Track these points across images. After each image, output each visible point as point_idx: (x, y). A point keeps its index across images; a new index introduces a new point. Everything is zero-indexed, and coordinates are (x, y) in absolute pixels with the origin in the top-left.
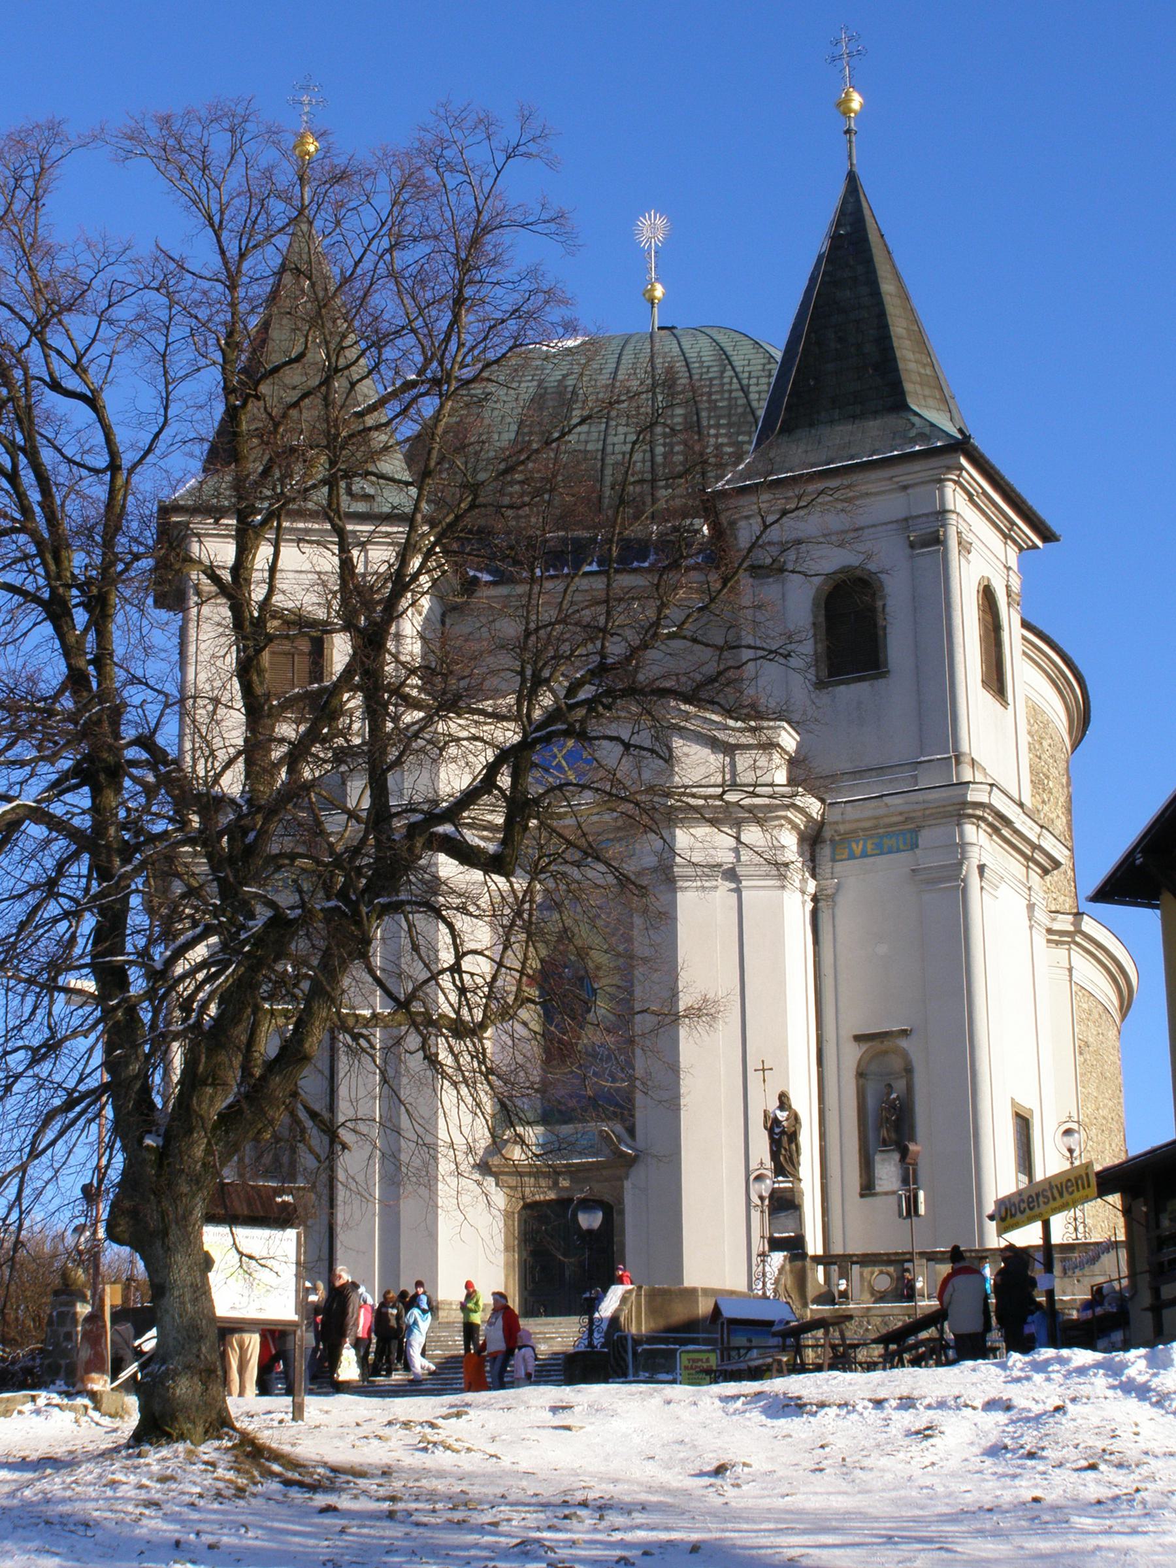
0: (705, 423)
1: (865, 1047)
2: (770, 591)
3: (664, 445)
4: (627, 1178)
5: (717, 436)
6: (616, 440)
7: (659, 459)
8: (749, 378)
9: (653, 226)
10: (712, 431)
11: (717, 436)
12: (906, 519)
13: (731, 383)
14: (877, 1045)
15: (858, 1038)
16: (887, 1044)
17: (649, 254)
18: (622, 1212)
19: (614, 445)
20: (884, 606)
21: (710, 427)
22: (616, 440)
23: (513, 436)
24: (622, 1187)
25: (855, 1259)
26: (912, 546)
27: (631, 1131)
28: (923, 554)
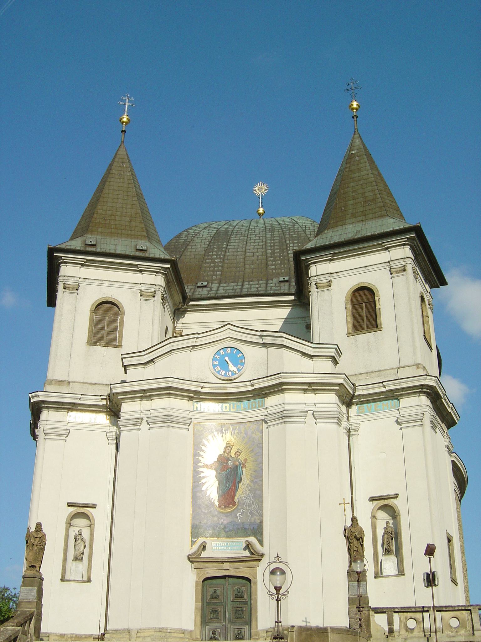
0: (288, 242)
1: (375, 503)
2: (325, 294)
3: (271, 249)
5: (294, 246)
6: (250, 248)
7: (269, 255)
8: (306, 227)
9: (261, 190)
10: (291, 245)
11: (294, 246)
12: (389, 262)
13: (298, 229)
14: (382, 503)
15: (372, 499)
16: (386, 502)
17: (259, 198)
18: (256, 583)
19: (249, 249)
20: (379, 299)
21: (290, 243)
22: (250, 248)
23: (206, 246)
25: (396, 610)
26: (391, 274)
27: (261, 542)
28: (397, 276)
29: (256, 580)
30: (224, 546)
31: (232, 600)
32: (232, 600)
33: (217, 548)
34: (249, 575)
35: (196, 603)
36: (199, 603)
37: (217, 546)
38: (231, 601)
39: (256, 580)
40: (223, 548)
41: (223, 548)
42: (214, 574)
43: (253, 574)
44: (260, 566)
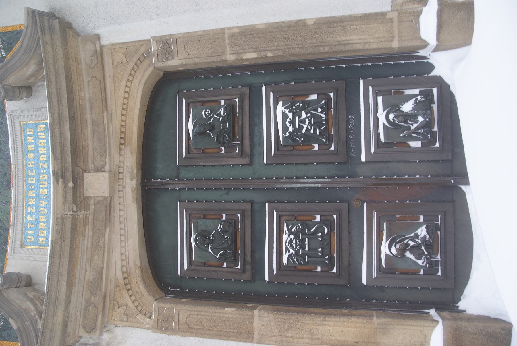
4: (98, 37)
24: (113, 47)
29: (154, 46)
30: (38, 197)
31: (246, 161)
32: (246, 161)
33: (43, 226)
34: (136, 82)
35: (256, 336)
36: (256, 323)
37: (37, 229)
38: (251, 163)
39: (154, 46)
40: (43, 203)
41: (43, 203)
42: (130, 241)
43: (131, 65)
44: (97, 32)
